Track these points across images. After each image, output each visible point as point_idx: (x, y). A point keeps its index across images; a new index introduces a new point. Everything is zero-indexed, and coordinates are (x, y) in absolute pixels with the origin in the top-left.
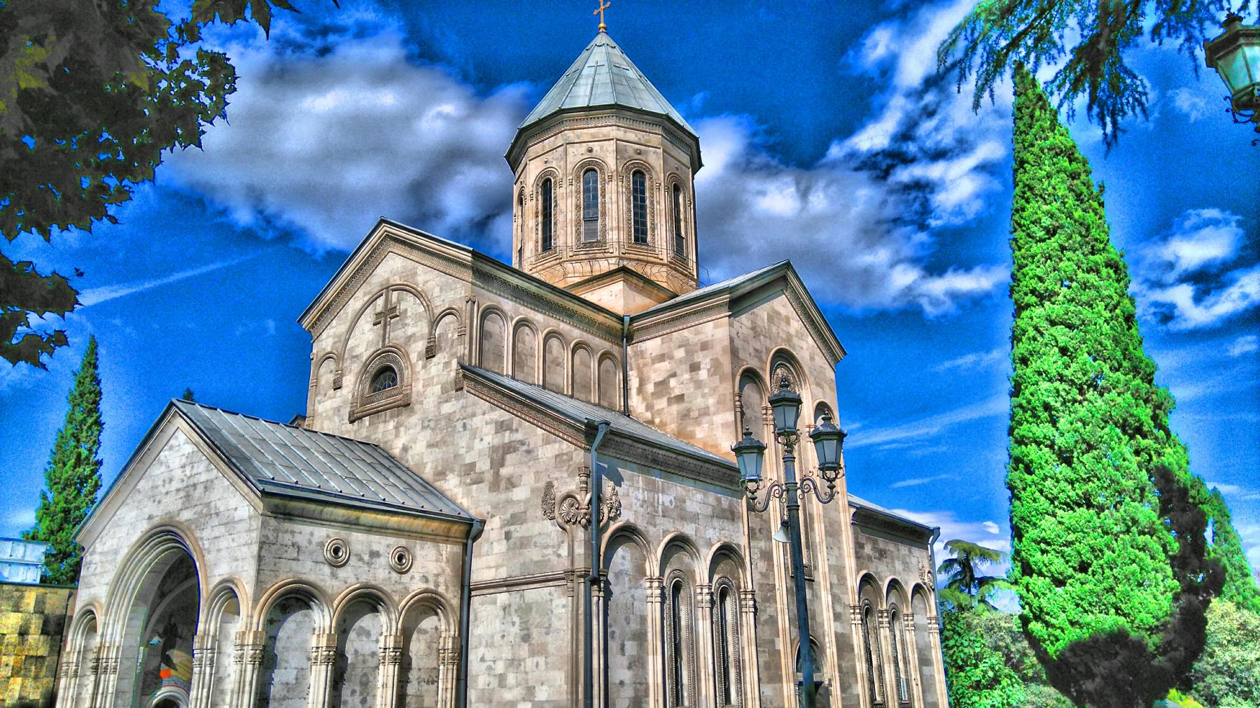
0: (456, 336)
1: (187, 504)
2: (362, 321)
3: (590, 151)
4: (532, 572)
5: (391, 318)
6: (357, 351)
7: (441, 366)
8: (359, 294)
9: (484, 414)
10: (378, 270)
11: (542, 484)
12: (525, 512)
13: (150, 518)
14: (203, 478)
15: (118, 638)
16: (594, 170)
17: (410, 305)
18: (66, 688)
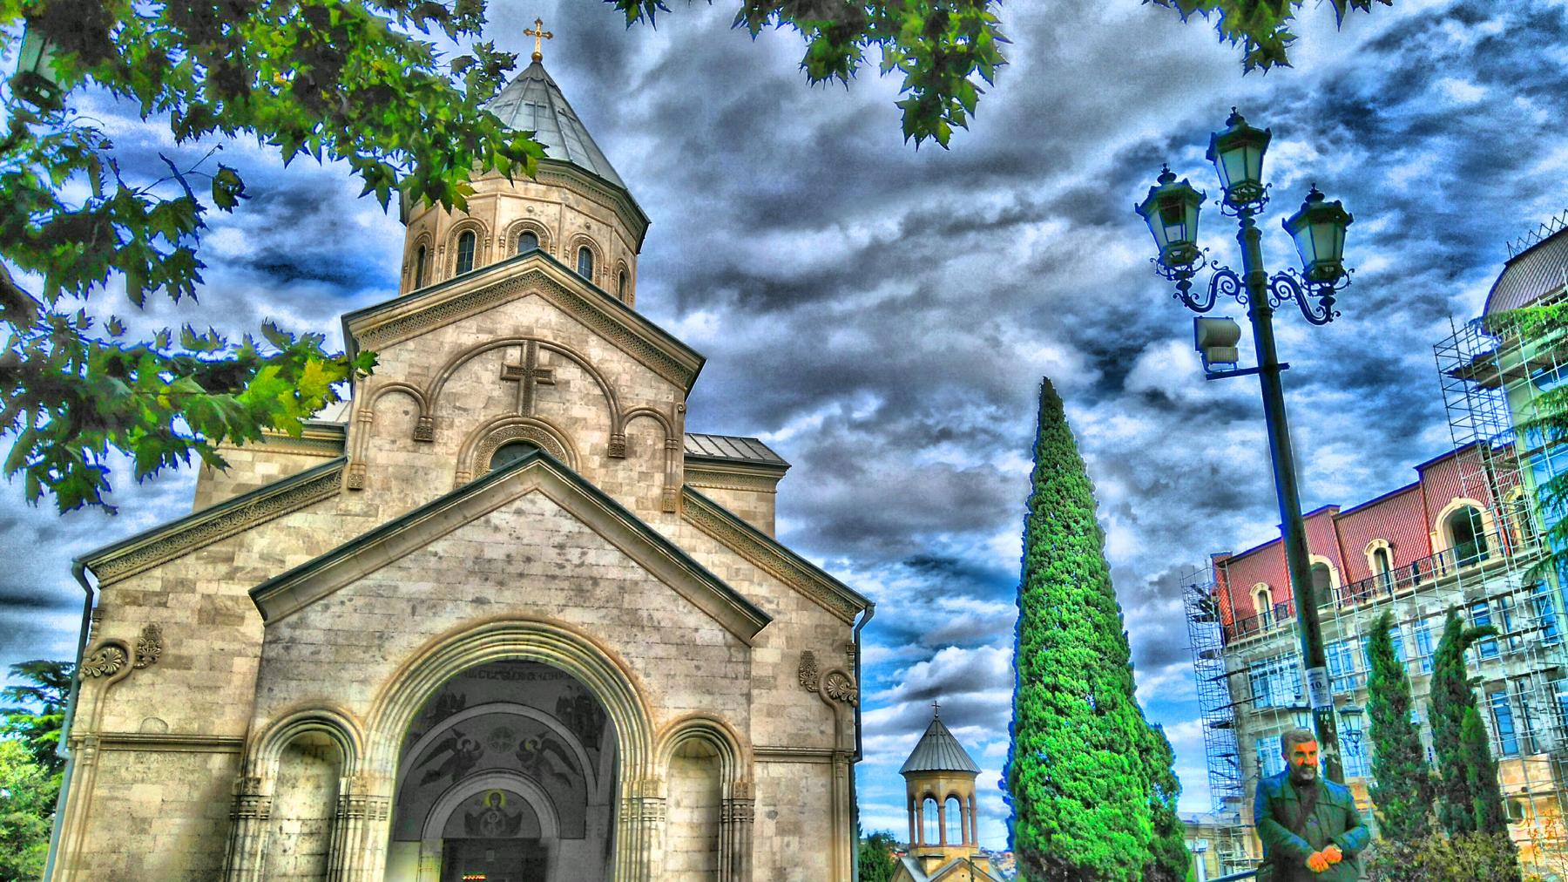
0: (661, 446)
1: (579, 600)
2: (475, 366)
3: (588, 228)
4: (785, 744)
5: (539, 382)
6: (469, 403)
7: (635, 475)
8: (472, 324)
9: (709, 552)
10: (509, 308)
11: (797, 652)
12: (775, 678)
13: (479, 601)
14: (614, 573)
15: (389, 768)
16: (535, 237)
17: (566, 372)
18: (255, 838)
